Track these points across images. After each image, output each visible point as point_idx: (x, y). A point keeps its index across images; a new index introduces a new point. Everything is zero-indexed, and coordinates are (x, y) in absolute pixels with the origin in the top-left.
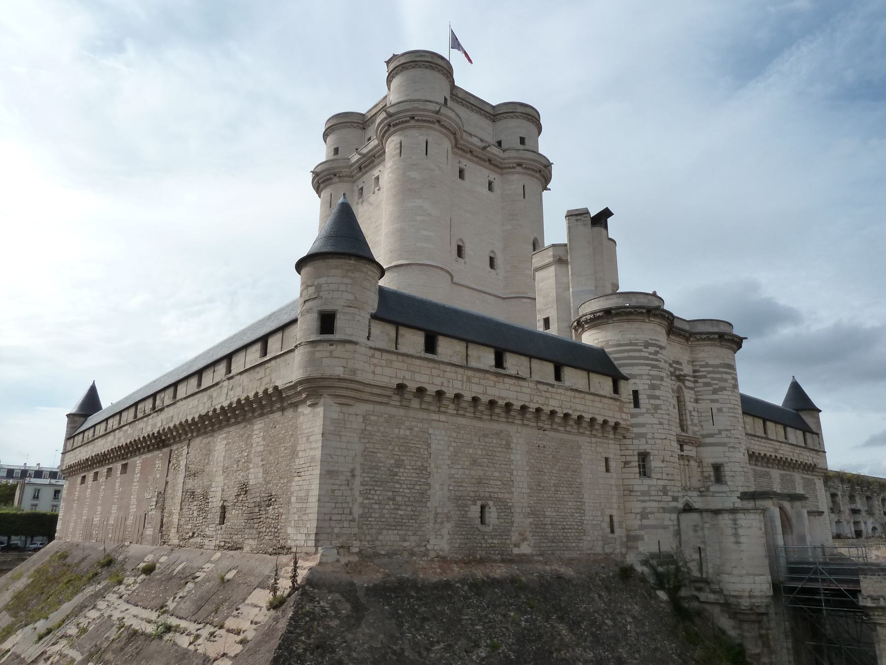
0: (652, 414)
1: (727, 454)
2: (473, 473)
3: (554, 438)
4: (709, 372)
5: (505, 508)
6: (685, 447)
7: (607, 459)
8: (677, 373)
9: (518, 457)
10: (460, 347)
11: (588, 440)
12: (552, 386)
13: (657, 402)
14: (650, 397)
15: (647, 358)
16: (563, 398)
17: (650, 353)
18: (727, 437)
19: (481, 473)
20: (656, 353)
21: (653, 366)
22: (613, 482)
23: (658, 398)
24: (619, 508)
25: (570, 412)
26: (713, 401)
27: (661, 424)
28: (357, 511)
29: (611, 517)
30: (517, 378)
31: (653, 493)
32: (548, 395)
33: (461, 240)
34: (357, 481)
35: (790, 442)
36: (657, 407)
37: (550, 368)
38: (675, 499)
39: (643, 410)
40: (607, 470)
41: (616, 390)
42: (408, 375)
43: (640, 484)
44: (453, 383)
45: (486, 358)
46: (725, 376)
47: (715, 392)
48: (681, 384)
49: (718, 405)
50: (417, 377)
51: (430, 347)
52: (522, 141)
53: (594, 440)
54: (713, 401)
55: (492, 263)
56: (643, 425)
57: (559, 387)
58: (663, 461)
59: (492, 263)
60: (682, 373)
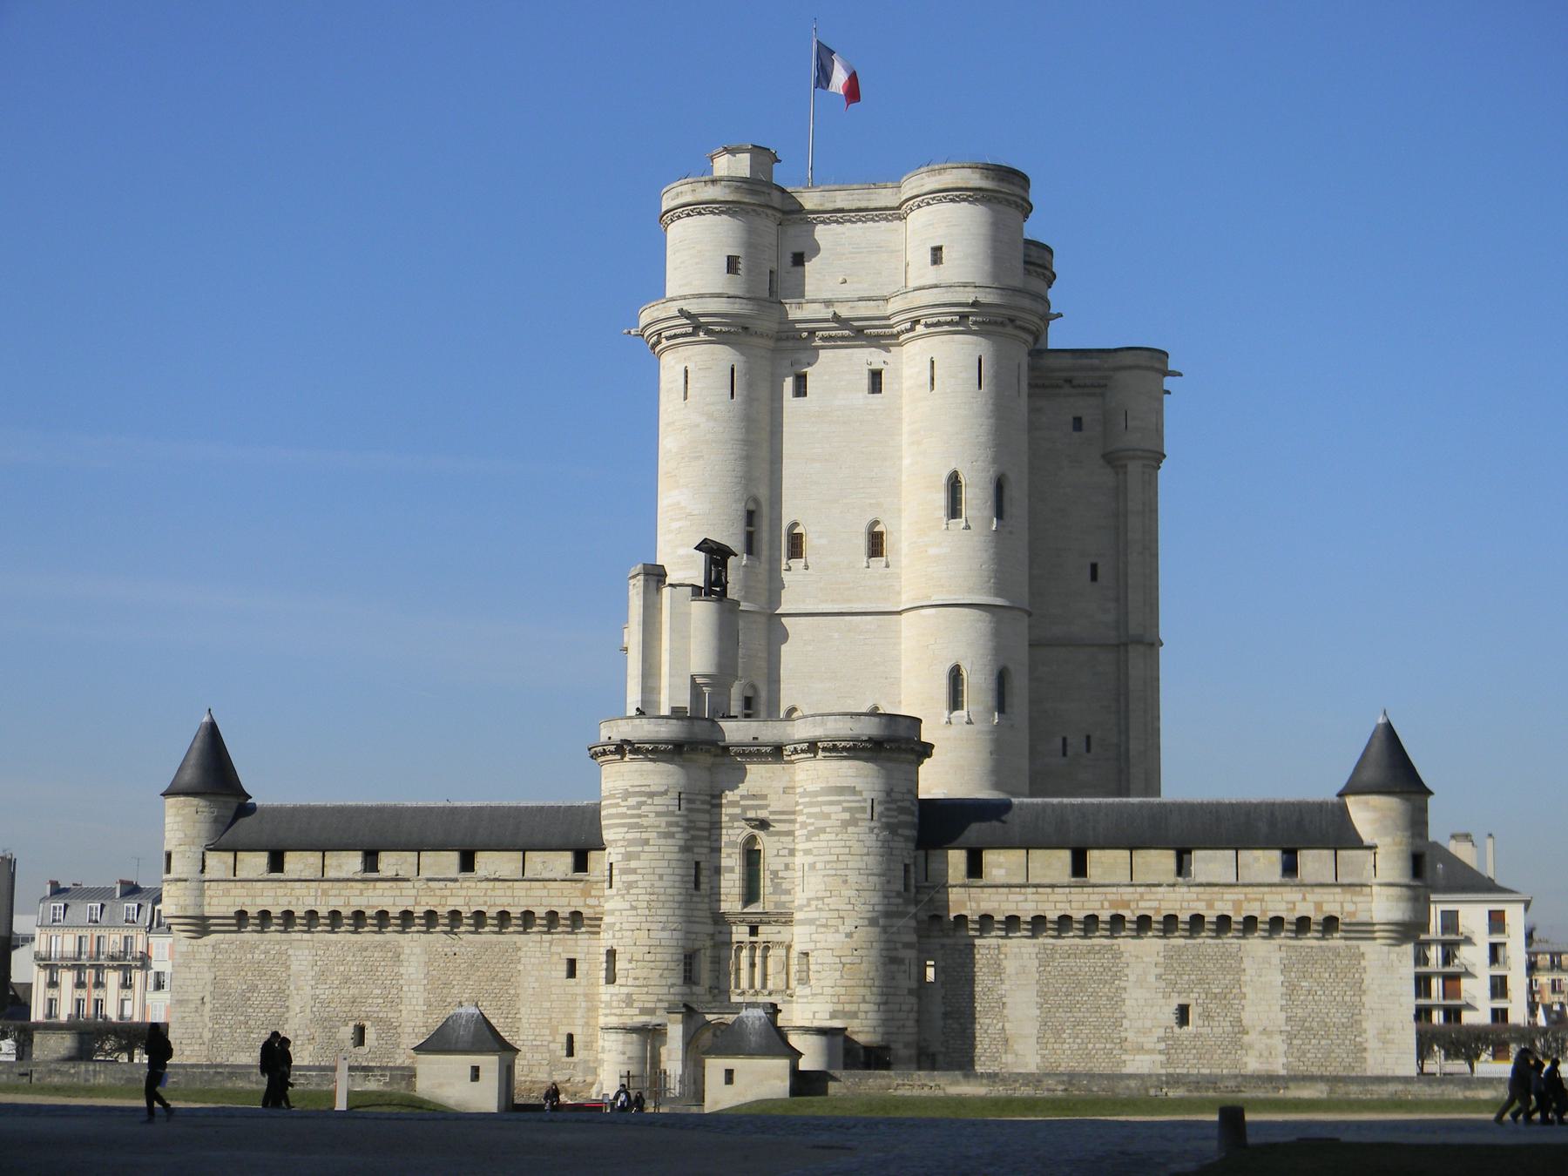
0: (623, 896)
1: (814, 937)
2: (344, 992)
3: (467, 941)
4: (806, 805)
5: (390, 1029)
6: (761, 929)
7: (572, 964)
8: (751, 814)
9: (411, 970)
10: (314, 858)
11: (537, 937)
12: (455, 880)
13: (632, 878)
14: (624, 872)
15: (624, 816)
16: (471, 892)
17: (629, 808)
18: (818, 909)
19: (354, 991)
20: (640, 805)
21: (631, 826)
22: (579, 990)
23: (634, 871)
24: (587, 1024)
25: (484, 909)
26: (807, 852)
27: (635, 908)
28: (207, 1035)
29: (570, 1037)
30: (396, 879)
31: (615, 1004)
32: (447, 892)
33: (795, 524)
34: (208, 1007)
35: (1198, 880)
36: (630, 886)
37: (453, 858)
38: (644, 1011)
39: (614, 891)
40: (572, 972)
41: (581, 864)
42: (248, 901)
43: (605, 992)
44: (302, 899)
45: (352, 862)
46: (826, 809)
47: (808, 839)
48: (756, 832)
49: (809, 859)
50: (259, 901)
51: (276, 864)
52: (937, 252)
53: (548, 937)
54: (807, 852)
55: (876, 545)
56: (612, 912)
57: (465, 880)
58: (630, 961)
59: (876, 545)
60: (762, 814)
